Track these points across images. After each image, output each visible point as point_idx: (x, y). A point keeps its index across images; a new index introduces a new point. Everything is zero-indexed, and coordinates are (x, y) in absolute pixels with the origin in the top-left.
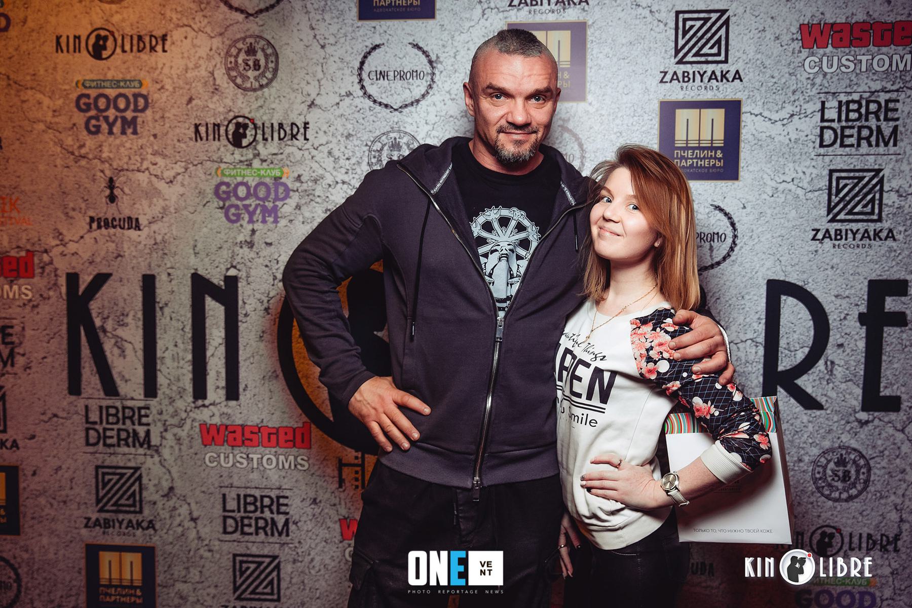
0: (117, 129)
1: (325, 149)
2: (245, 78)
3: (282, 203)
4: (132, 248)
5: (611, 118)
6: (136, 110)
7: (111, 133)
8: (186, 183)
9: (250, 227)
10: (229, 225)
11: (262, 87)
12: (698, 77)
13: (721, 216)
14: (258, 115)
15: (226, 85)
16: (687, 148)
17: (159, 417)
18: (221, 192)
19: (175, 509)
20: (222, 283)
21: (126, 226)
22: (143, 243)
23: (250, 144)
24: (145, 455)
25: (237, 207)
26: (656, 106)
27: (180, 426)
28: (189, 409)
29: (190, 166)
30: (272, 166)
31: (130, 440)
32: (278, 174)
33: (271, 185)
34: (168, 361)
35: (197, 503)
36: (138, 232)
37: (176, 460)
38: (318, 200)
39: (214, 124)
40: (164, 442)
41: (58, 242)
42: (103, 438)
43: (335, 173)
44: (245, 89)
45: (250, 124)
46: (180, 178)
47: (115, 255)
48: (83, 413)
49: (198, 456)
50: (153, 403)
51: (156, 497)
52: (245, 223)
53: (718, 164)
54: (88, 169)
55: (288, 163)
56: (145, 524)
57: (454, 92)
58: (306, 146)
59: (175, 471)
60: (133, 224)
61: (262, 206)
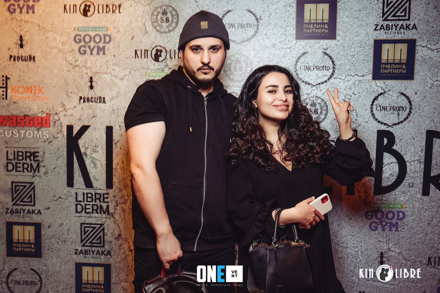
2: (161, 27)
5: (349, 48)
7: (91, 54)
8: (130, 79)
11: (170, 31)
12: (394, 27)
13: (403, 98)
14: (168, 45)
15: (151, 30)
16: (387, 64)
17: (114, 198)
19: (121, 245)
26: (372, 42)
27: (125, 203)
29: (132, 71)
31: (99, 210)
36: (104, 104)
41: (63, 109)
42: (84, 209)
44: (161, 32)
46: (126, 77)
47: (92, 116)
48: (75, 196)
50: (111, 191)
51: (112, 239)
53: (403, 72)
54: (79, 72)
56: (106, 253)
57: (268, 34)
60: (102, 100)
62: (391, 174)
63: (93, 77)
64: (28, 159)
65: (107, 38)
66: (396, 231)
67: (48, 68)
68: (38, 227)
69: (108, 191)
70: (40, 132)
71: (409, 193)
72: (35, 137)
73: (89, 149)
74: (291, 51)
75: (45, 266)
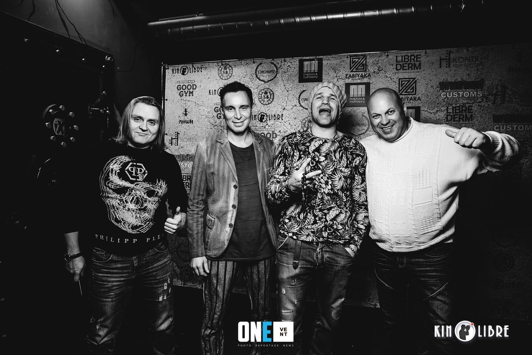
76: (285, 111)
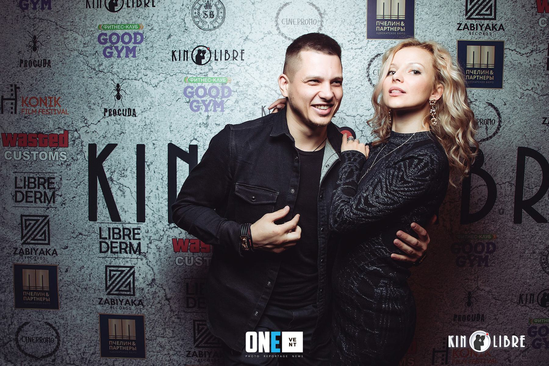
0: (123, 54)
1: (254, 66)
3: (226, 99)
4: (131, 128)
6: (134, 43)
7: (119, 56)
9: (206, 114)
10: (193, 113)
13: (492, 109)
14: (212, 45)
17: (146, 234)
18: (187, 93)
20: (188, 150)
21: (127, 114)
22: (138, 124)
23: (207, 62)
24: (137, 258)
25: (198, 102)
26: (456, 44)
28: (165, 229)
29: (168, 76)
30: (220, 76)
31: (128, 249)
32: (224, 81)
33: (220, 88)
34: (152, 199)
35: (170, 289)
37: (157, 261)
38: (249, 97)
39: (185, 51)
40: (149, 250)
41: (85, 125)
42: (110, 248)
43: (260, 81)
45: (207, 51)
46: (161, 84)
47: (119, 132)
49: (171, 259)
50: (142, 225)
51: (143, 286)
52: (202, 111)
53: (491, 78)
54: (104, 79)
55: (231, 74)
56: (137, 302)
58: (242, 64)
59: (155, 268)
60: (132, 112)
61: (213, 101)
62: (480, 199)
63: (120, 85)
64: (41, 187)
65: (139, 37)
66: (485, 266)
67: (66, 75)
68: (53, 270)
69: (139, 225)
70: (56, 153)
71: (500, 221)
72: (50, 159)
73: (116, 173)
74: (362, 52)
75: (63, 319)
76: (249, 43)
